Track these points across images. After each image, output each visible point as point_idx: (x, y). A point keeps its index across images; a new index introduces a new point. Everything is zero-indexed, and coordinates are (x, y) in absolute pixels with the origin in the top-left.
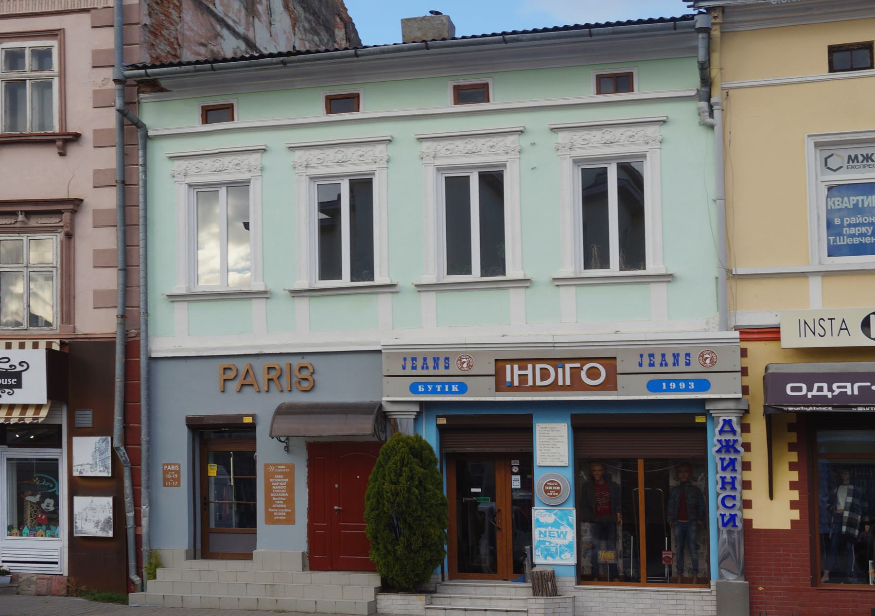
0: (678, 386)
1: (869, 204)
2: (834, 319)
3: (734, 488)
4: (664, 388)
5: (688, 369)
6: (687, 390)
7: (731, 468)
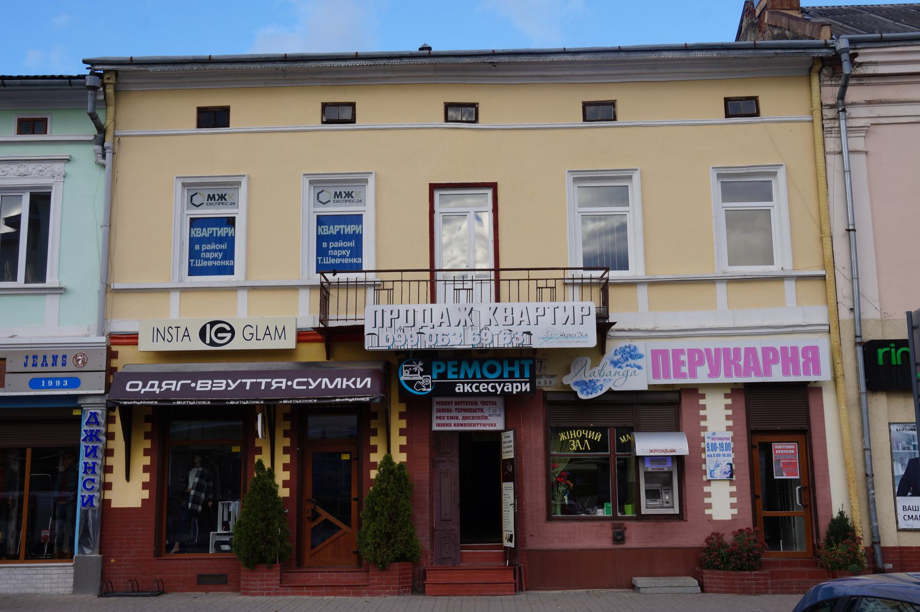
0: (54, 384)
1: (232, 235)
2: (180, 327)
3: (94, 472)
4: (43, 385)
5: (64, 369)
6: (61, 387)
7: (92, 454)
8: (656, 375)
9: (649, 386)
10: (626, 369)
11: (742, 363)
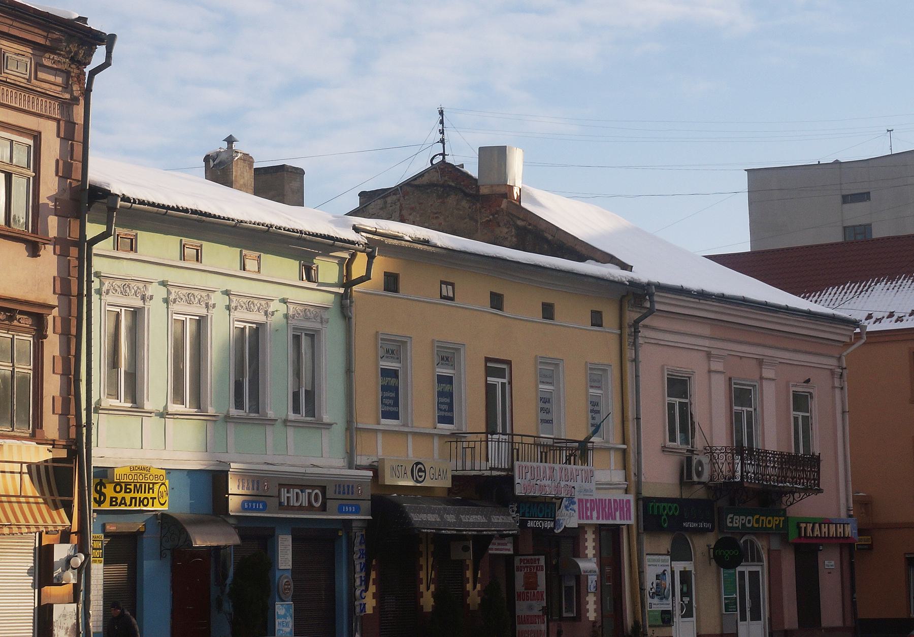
8: (580, 518)
9: (578, 524)
10: (571, 511)
11: (607, 510)
